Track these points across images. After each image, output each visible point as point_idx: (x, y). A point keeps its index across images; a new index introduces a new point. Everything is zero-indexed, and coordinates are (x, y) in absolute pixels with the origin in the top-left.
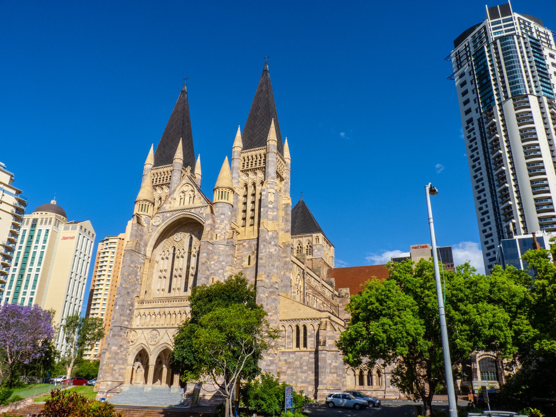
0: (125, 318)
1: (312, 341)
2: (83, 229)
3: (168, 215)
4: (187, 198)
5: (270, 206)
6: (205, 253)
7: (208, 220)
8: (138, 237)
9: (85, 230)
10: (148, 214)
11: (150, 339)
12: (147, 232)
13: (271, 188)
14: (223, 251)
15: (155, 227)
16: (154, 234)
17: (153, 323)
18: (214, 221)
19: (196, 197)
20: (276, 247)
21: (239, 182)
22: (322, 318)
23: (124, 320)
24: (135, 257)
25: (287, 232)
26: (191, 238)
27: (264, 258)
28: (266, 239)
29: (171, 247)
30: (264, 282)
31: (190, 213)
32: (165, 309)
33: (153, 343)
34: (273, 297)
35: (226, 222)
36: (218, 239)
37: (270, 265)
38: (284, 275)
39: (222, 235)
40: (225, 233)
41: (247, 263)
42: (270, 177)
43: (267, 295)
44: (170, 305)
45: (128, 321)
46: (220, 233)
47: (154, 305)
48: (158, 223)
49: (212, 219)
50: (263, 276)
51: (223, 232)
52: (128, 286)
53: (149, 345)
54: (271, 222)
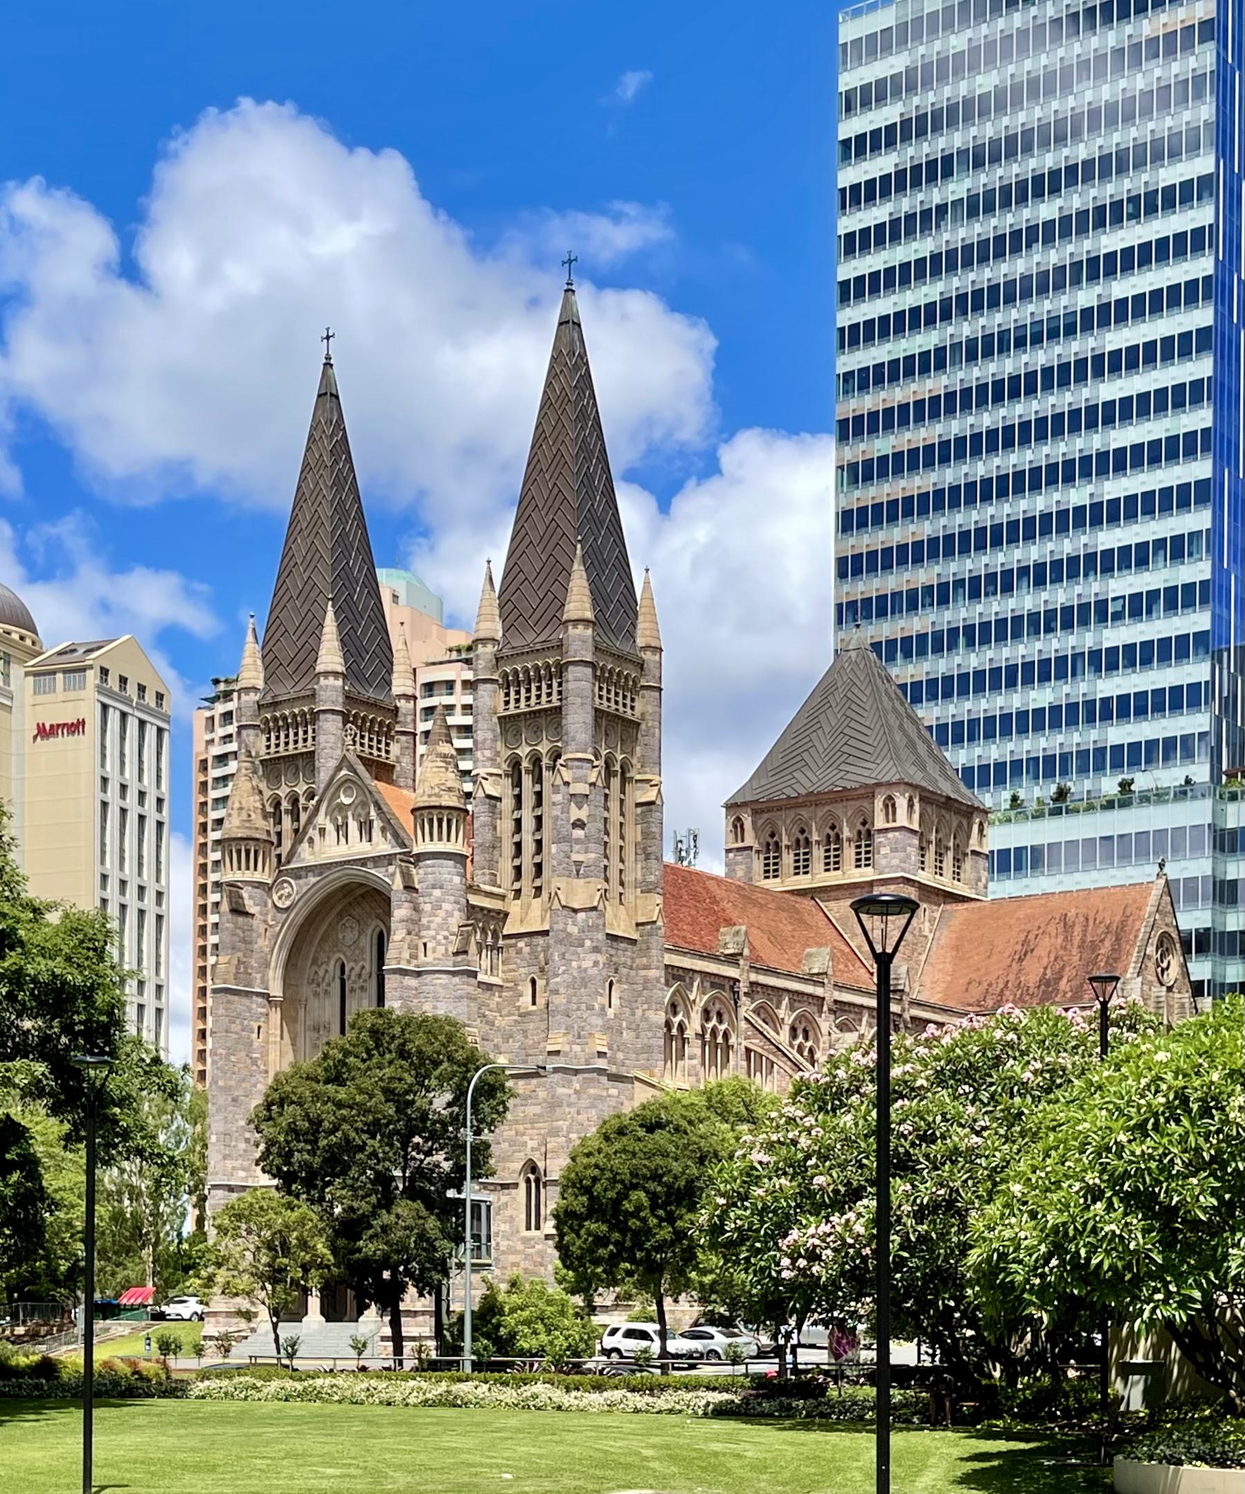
0: (238, 1163)
2: (113, 683)
5: (579, 833)
8: (239, 950)
9: (123, 680)
10: (258, 876)
12: (262, 927)
13: (577, 780)
14: (444, 987)
18: (416, 909)
20: (594, 956)
21: (498, 754)
23: (234, 1168)
24: (239, 1003)
25: (649, 891)
27: (562, 990)
28: (570, 935)
29: (332, 963)
30: (566, 1054)
34: (592, 1091)
35: (446, 906)
36: (430, 958)
37: (583, 1007)
38: (644, 1019)
39: (439, 944)
40: (446, 938)
41: (530, 999)
42: (572, 746)
43: (577, 1086)
45: (244, 1169)
46: (434, 938)
48: (288, 903)
49: (411, 902)
50: (560, 1040)
51: (440, 937)
52: (232, 1083)
54: (582, 881)
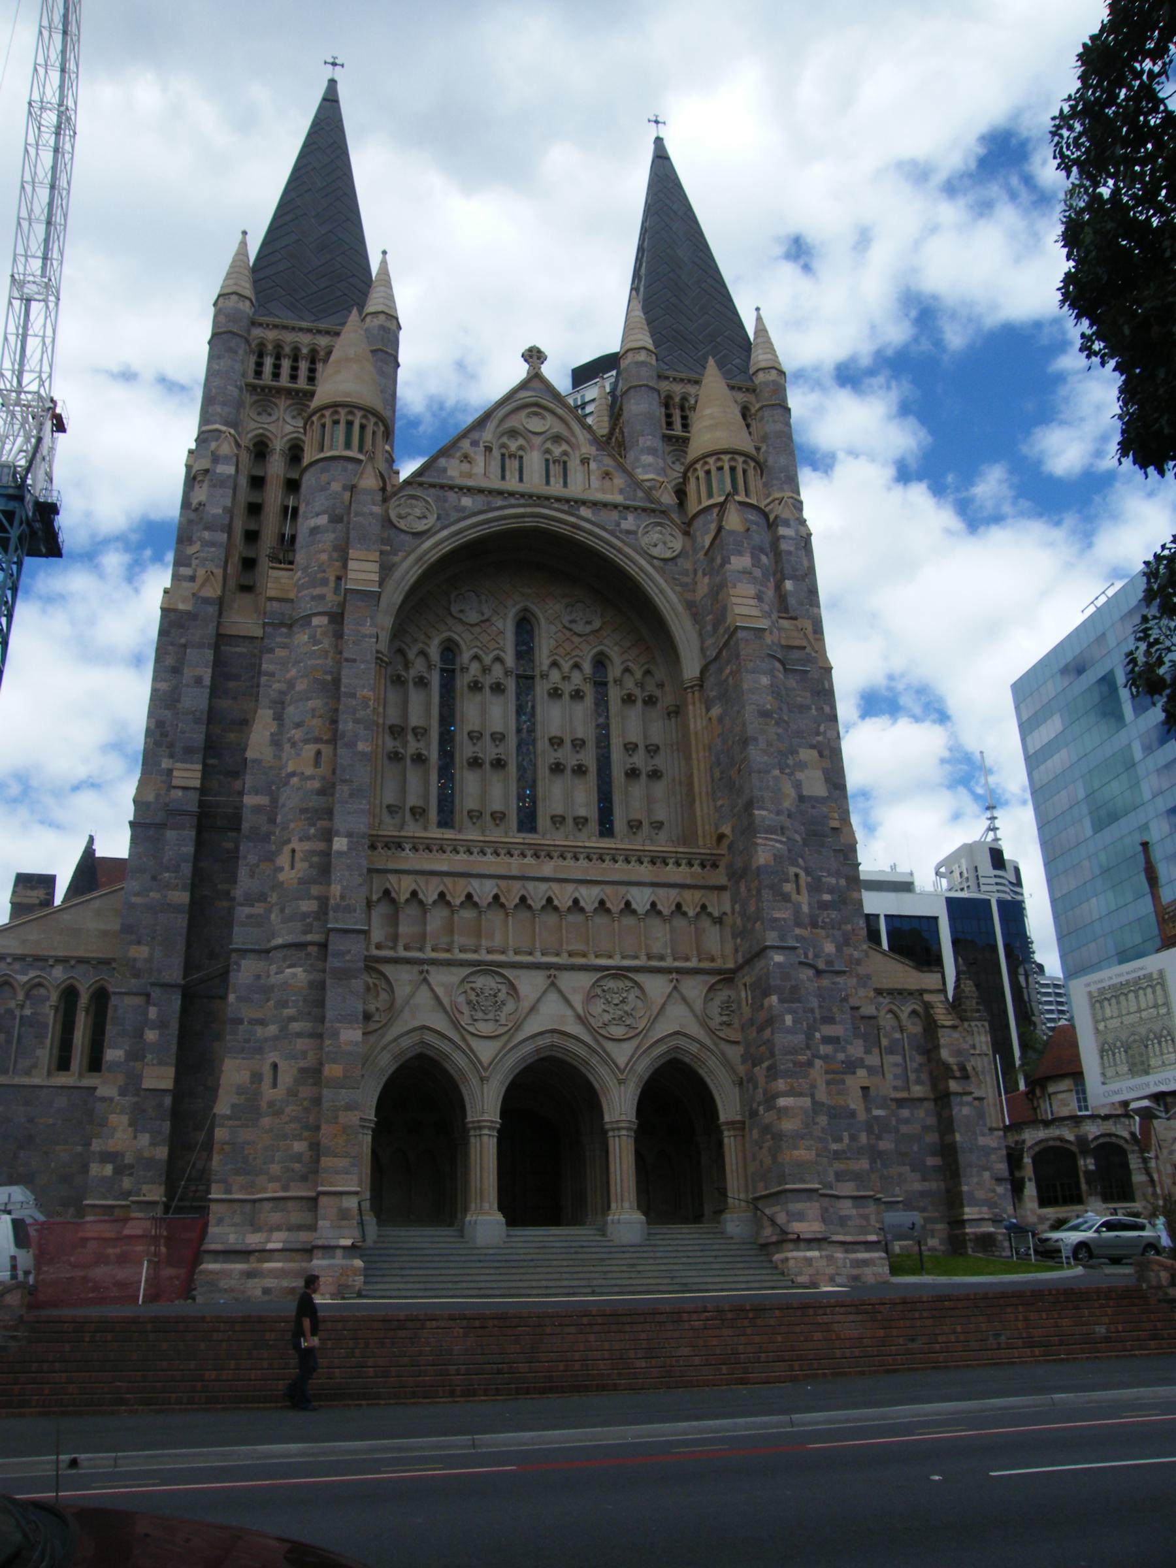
1: (896, 1065)
3: (466, 501)
4: (534, 461)
6: (765, 674)
7: (740, 553)
11: (465, 1009)
15: (403, 536)
16: (405, 565)
17: (469, 942)
19: (593, 465)
22: (926, 991)
26: (525, 626)
31: (572, 519)
32: (530, 885)
33: (485, 1028)
44: (548, 868)
46: (770, 617)
47: (459, 862)
48: (421, 526)
53: (468, 1037)
